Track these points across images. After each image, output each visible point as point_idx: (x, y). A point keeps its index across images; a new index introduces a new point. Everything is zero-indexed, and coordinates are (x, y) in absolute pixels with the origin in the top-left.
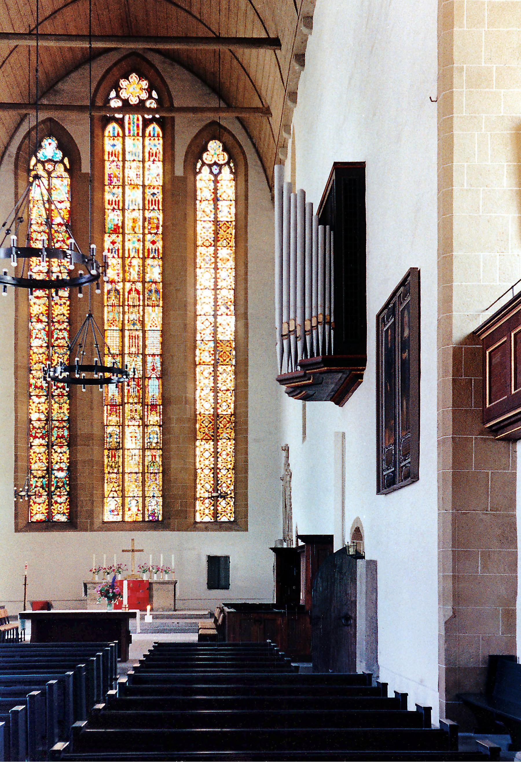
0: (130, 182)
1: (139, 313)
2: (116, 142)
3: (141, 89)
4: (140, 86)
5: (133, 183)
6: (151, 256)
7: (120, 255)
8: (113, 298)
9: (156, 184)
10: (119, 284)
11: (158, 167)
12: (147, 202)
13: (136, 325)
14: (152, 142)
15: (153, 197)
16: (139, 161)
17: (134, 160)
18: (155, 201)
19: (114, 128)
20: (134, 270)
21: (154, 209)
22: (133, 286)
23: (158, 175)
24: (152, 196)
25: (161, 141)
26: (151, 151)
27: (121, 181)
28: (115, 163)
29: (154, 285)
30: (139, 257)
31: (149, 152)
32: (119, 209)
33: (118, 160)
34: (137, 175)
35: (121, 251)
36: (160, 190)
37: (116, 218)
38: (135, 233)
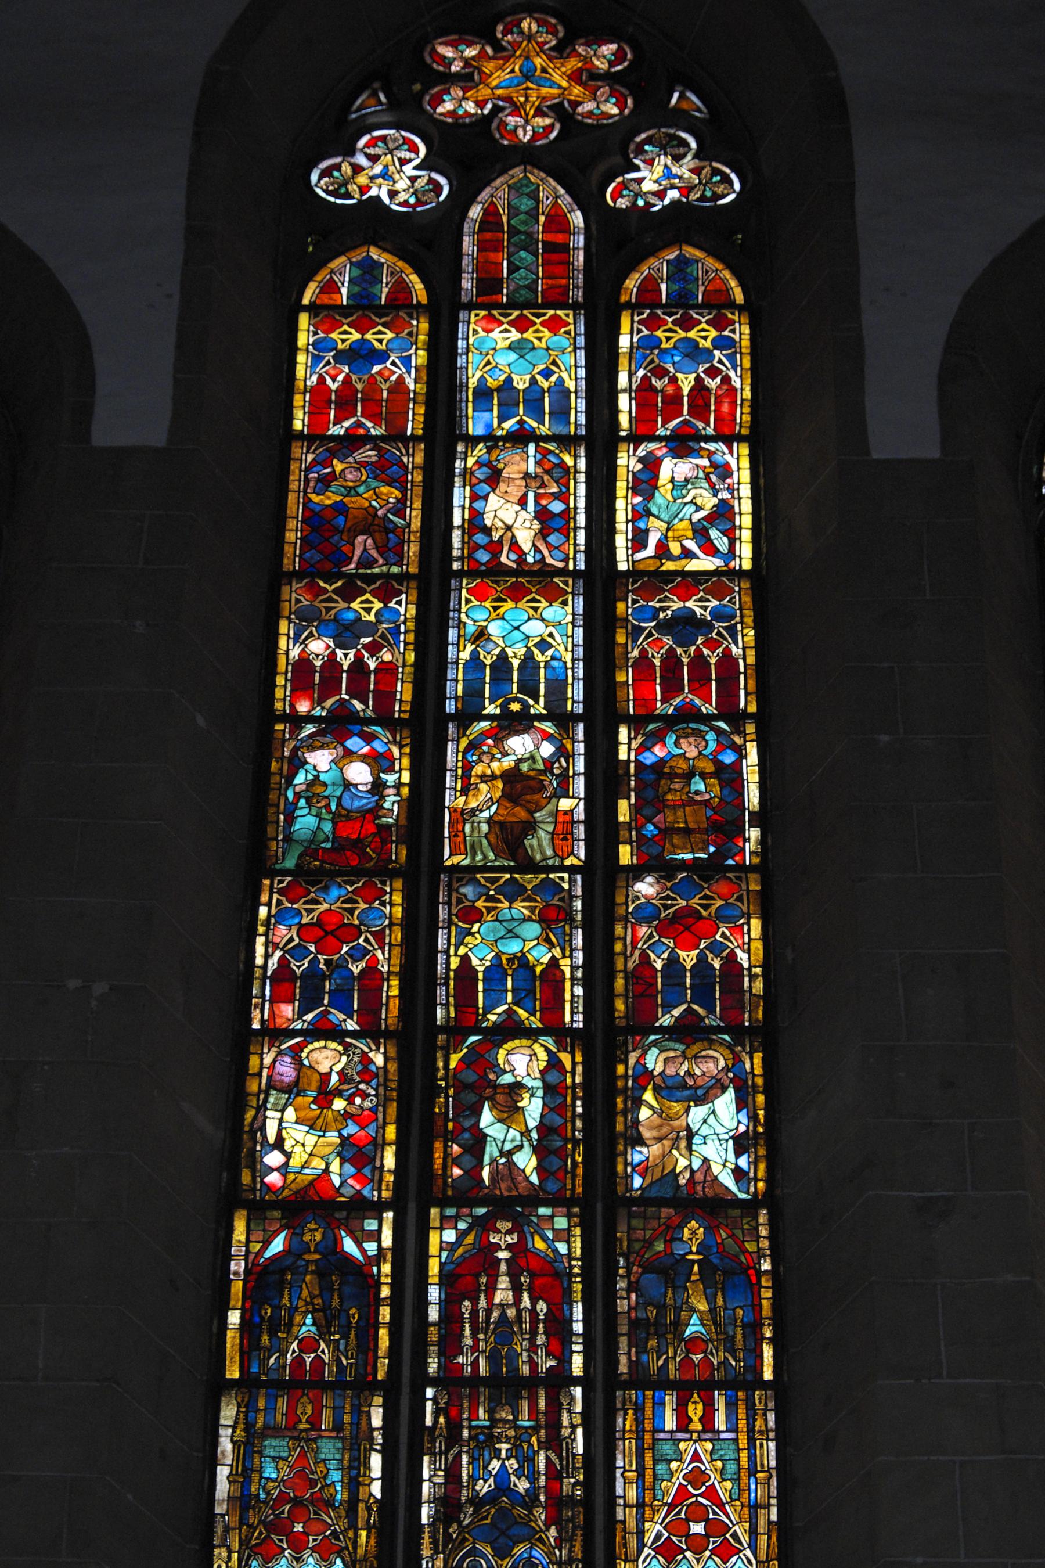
0: (483, 557)
1: (555, 1441)
2: (381, 337)
3: (588, 77)
4: (573, 63)
5: (507, 559)
6: (666, 1021)
7: (391, 1013)
8: (307, 1327)
9: (705, 563)
10: (371, 1225)
11: (725, 471)
12: (625, 676)
13: (534, 1538)
14: (668, 336)
15: (685, 644)
16: (566, 442)
17: (521, 438)
18: (699, 663)
19: (369, 270)
20: (510, 1112)
21: (688, 715)
22: (503, 1238)
23: (723, 513)
24: (668, 641)
25: (742, 332)
26: (657, 383)
27: (413, 549)
28: (369, 454)
29: (693, 1232)
30: (554, 1027)
31: (643, 393)
32: (385, 718)
33: (396, 436)
34: (542, 515)
35: (393, 988)
36: (740, 597)
37: (360, 773)
38: (530, 866)
